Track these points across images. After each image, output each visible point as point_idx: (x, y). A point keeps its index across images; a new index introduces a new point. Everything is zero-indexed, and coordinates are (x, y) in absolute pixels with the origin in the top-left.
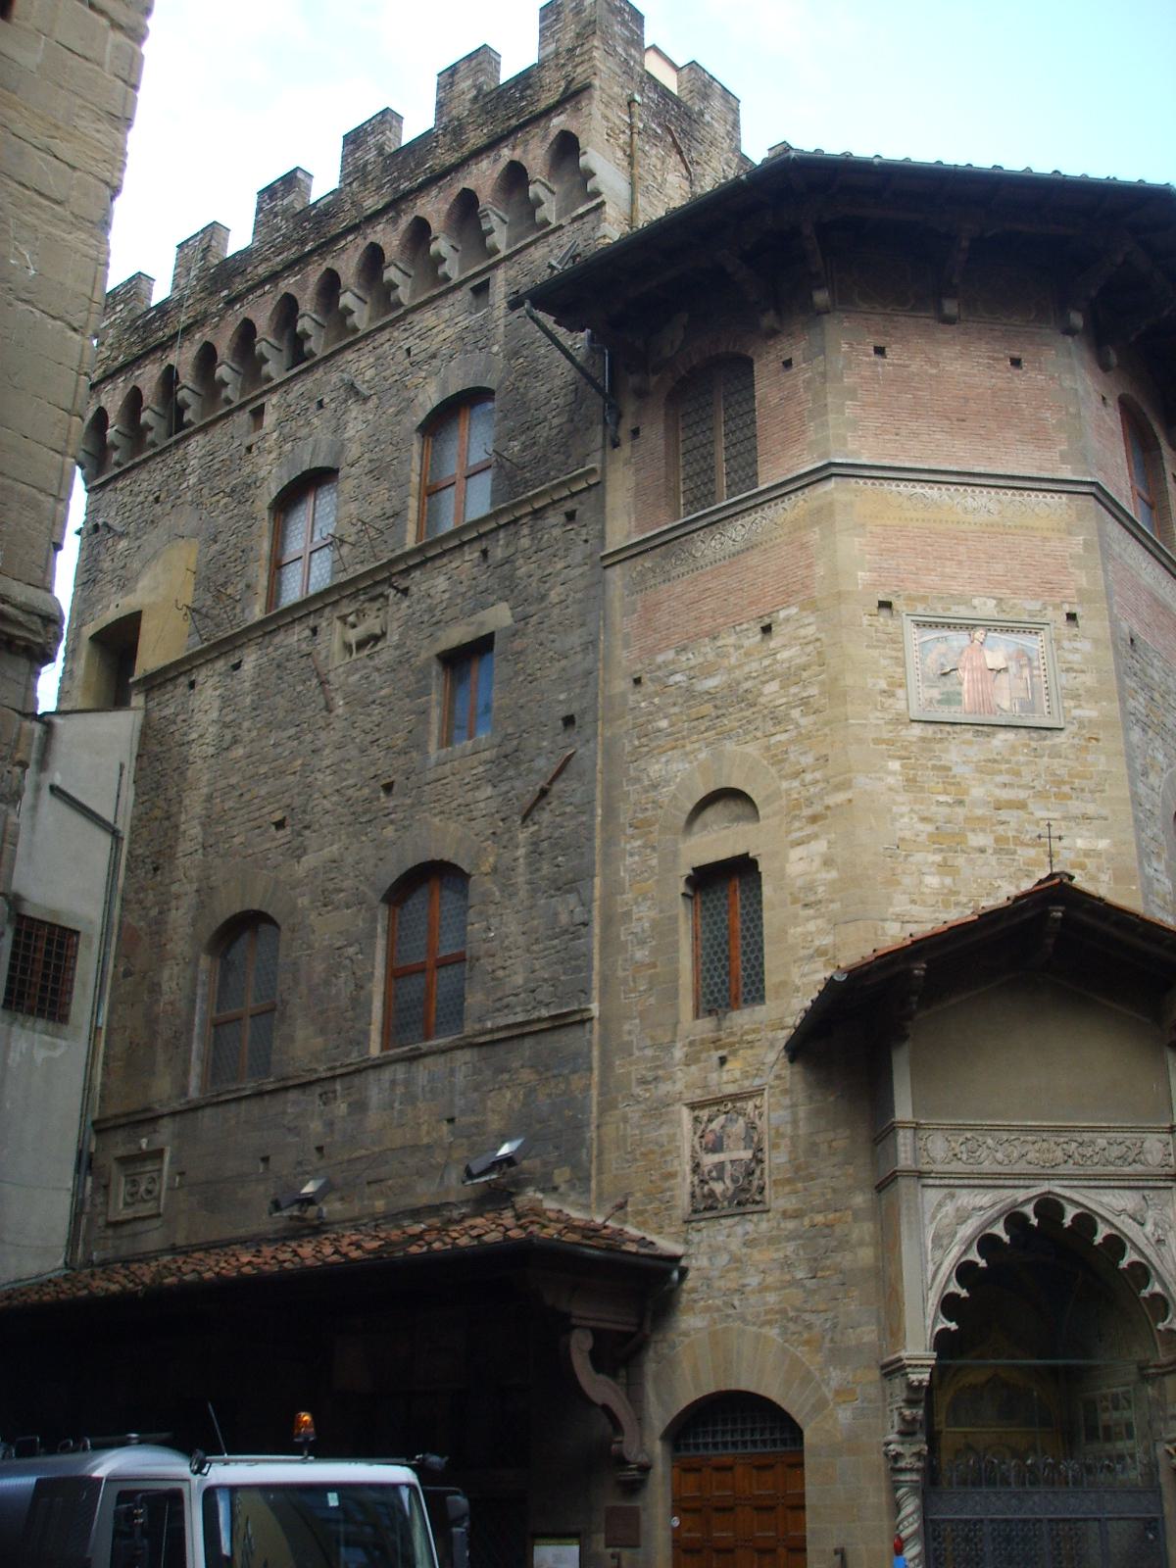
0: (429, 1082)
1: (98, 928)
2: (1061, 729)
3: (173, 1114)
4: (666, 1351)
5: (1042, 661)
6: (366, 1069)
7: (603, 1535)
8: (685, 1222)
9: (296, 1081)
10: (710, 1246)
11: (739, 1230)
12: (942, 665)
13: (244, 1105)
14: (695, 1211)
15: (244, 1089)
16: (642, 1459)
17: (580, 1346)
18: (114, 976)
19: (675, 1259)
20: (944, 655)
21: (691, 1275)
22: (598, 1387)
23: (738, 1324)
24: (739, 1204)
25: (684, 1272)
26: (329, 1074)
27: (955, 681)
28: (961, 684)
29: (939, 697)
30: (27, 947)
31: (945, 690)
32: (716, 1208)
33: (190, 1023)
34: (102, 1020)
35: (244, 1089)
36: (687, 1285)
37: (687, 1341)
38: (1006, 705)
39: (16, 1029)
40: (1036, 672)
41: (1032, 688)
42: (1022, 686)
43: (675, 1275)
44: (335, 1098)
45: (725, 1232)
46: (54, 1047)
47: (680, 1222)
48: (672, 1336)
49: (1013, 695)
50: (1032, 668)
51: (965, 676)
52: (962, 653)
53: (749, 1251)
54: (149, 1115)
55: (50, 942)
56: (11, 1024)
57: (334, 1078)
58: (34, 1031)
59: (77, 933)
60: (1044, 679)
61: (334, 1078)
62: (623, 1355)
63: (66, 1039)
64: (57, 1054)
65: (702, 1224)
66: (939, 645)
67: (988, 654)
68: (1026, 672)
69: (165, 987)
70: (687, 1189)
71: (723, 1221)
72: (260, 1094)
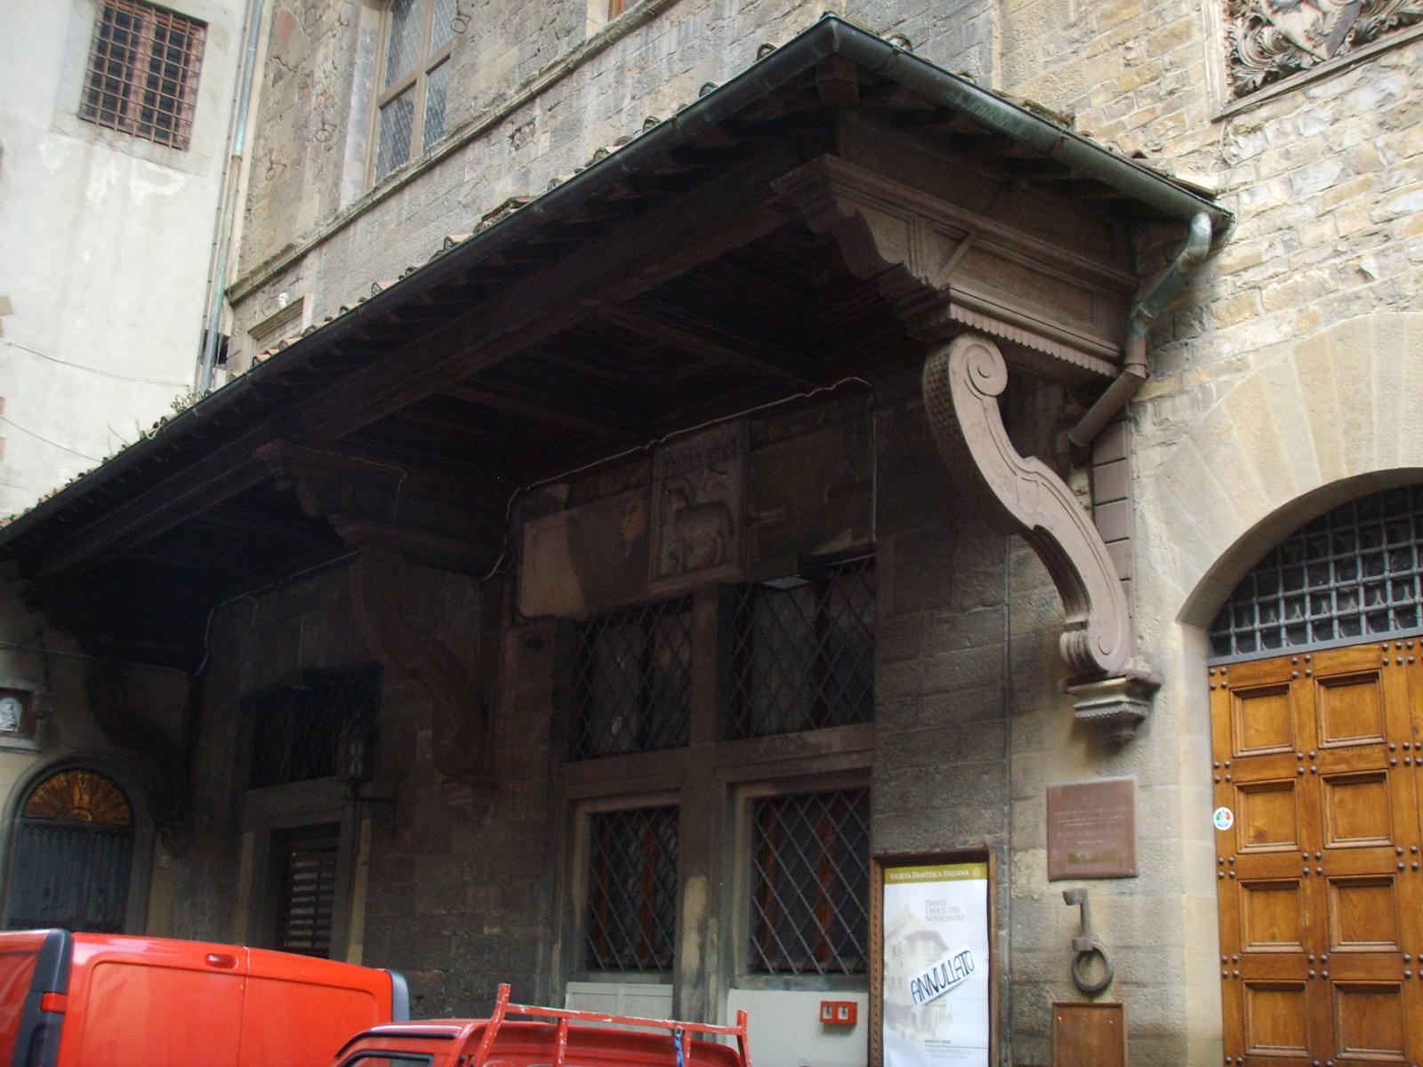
0: (679, 43)
1: (238, 21)
3: (322, 242)
4: (1185, 415)
6: (578, 64)
7: (1043, 853)
8: (1216, 121)
9: (478, 126)
10: (1287, 155)
11: (1365, 98)
13: (407, 194)
14: (1241, 93)
15: (406, 169)
16: (1141, 667)
17: (973, 383)
18: (264, 87)
19: (1208, 196)
21: (1238, 231)
22: (1025, 488)
23: (1384, 312)
24: (1357, 43)
25: (1222, 224)
26: (524, 95)
30: (120, 36)
32: (1299, 68)
33: (346, 106)
34: (245, 144)
35: (406, 169)
36: (1230, 257)
37: (1239, 380)
39: (101, 149)
43: (1203, 225)
44: (533, 133)
45: (1326, 114)
46: (165, 181)
47: (1207, 123)
48: (1197, 376)
53: (1396, 136)
54: (292, 255)
55: (160, 34)
56: (92, 142)
57: (531, 99)
58: (131, 154)
59: (203, 25)
61: (531, 99)
62: (1078, 419)
63: (183, 171)
64: (168, 191)
65: (1263, 112)
69: (319, 74)
70: (1220, 50)
71: (1315, 90)
72: (429, 168)
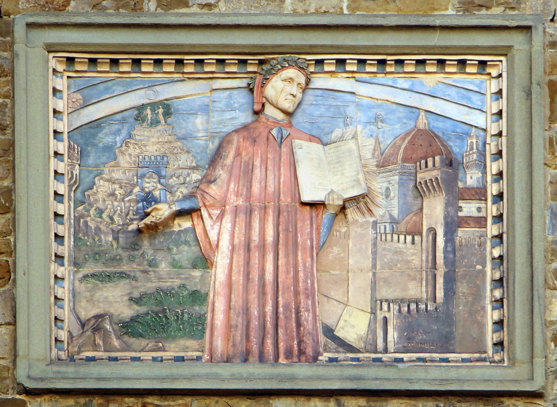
2: (537, 395)
5: (493, 168)
12: (149, 199)
20: (157, 167)
27: (186, 253)
28: (205, 262)
29: (127, 312)
31: (150, 286)
38: (354, 326)
40: (469, 208)
41: (450, 264)
42: (414, 254)
49: (384, 293)
50: (456, 194)
51: (220, 232)
52: (216, 158)
60: (492, 230)
66: (142, 133)
67: (306, 152)
68: (435, 210)
